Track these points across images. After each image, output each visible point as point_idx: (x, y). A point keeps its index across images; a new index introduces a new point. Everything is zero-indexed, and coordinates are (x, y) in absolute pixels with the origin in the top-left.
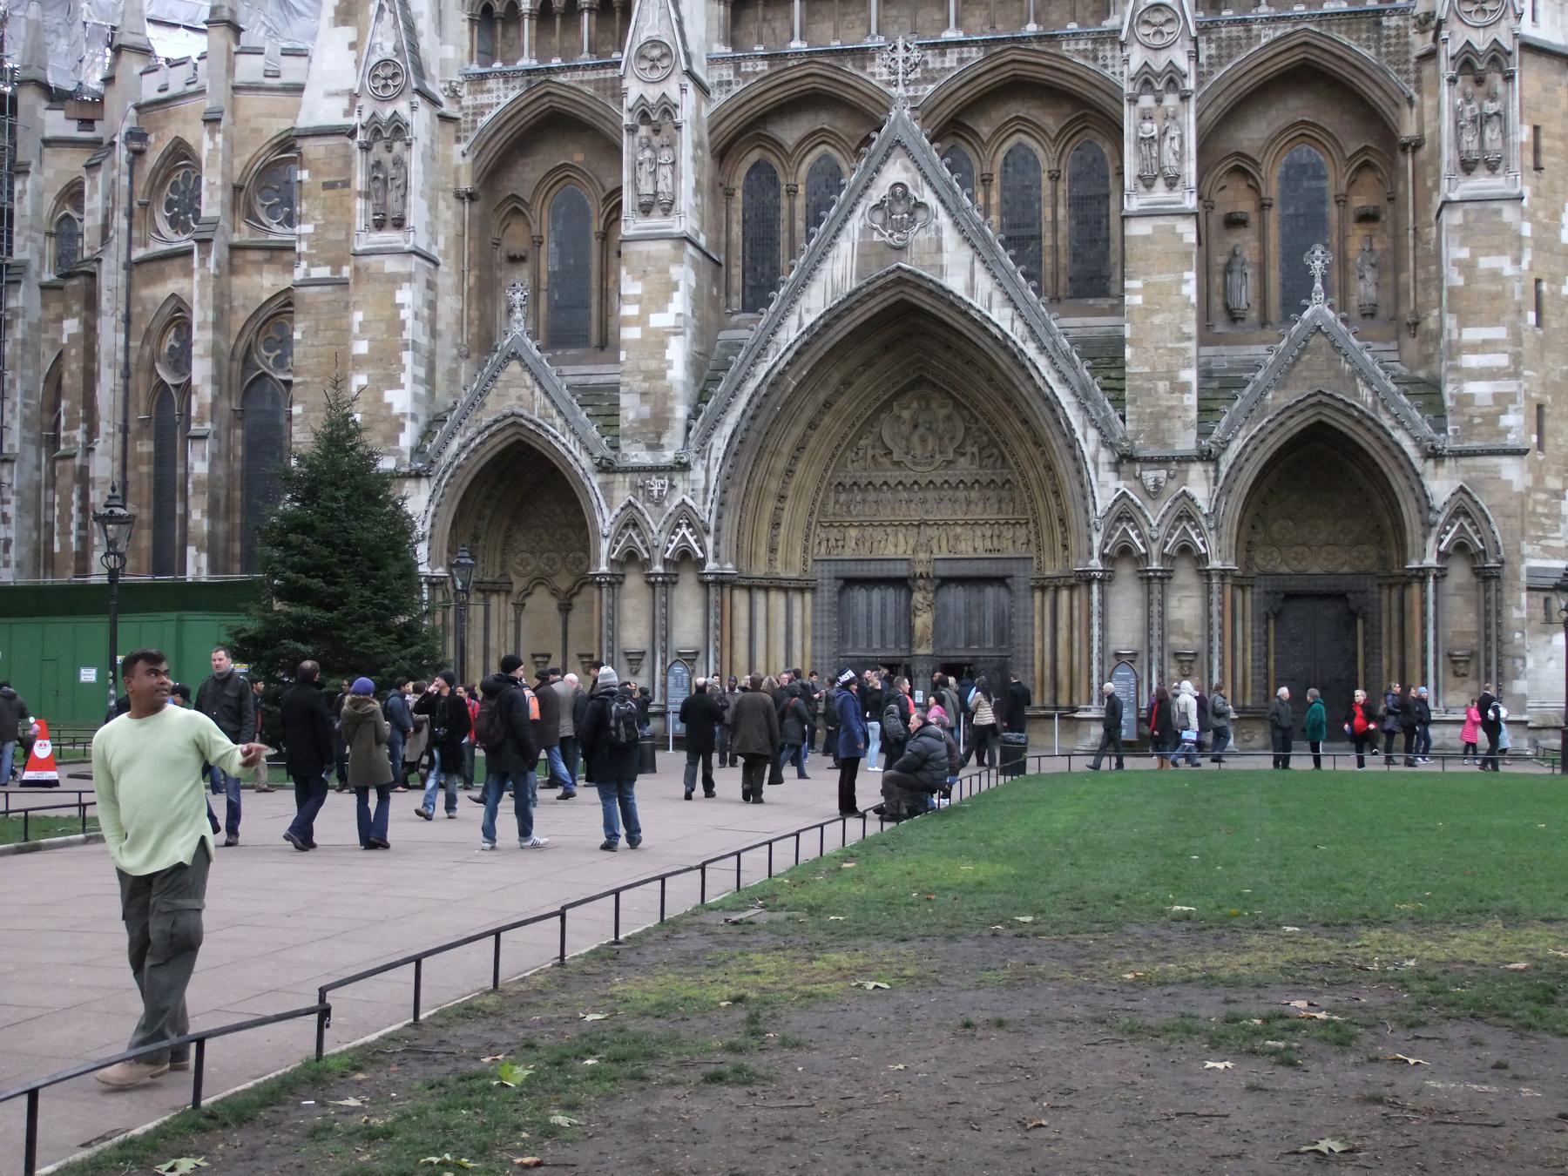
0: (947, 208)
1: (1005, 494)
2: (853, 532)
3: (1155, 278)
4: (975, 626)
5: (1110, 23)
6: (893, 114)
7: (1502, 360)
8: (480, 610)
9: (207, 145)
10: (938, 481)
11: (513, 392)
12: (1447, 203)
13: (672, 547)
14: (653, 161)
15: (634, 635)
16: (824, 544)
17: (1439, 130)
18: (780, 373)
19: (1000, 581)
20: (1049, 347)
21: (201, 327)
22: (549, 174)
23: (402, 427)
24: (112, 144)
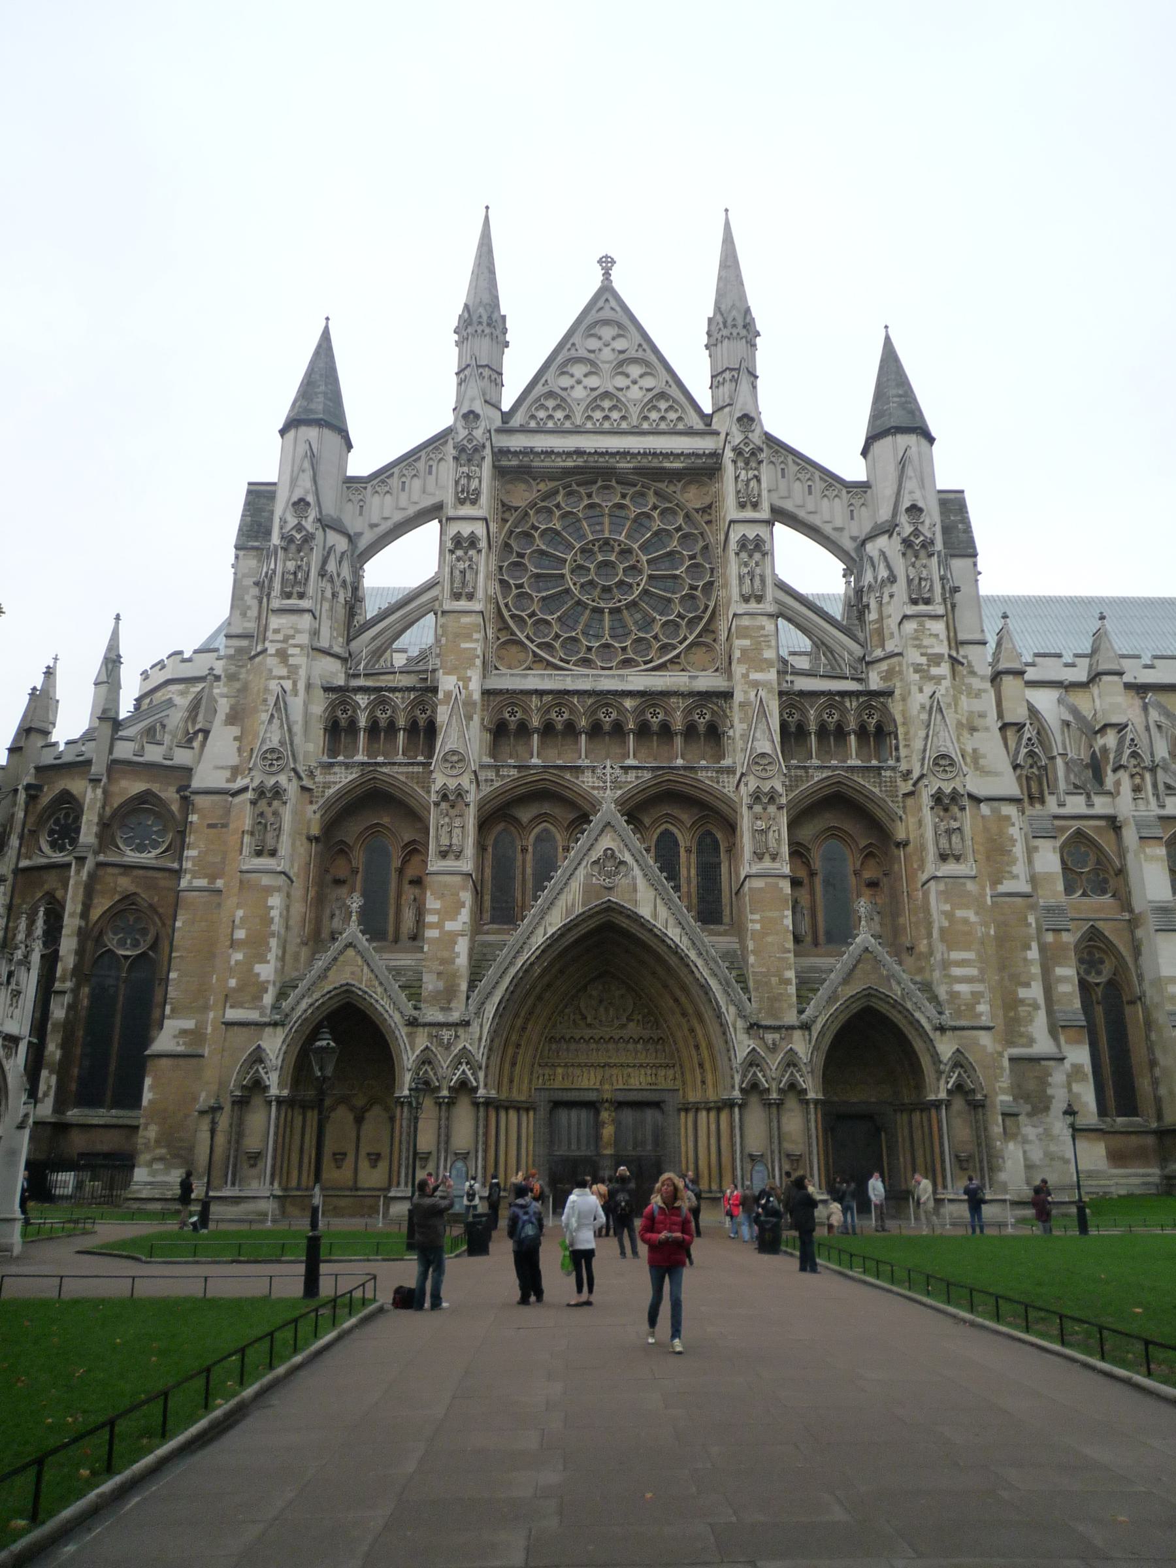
1: (659, 1047)
2: (560, 1070)
3: (769, 914)
5: (726, 762)
6: (604, 805)
7: (973, 972)
8: (301, 1118)
9: (91, 798)
10: (617, 1037)
11: (348, 969)
12: (934, 878)
13: (455, 1078)
15: (426, 1140)
16: (541, 1078)
17: (922, 836)
19: (657, 1105)
20: (704, 953)
21: (72, 915)
22: (366, 829)
23: (266, 991)
24: (16, 791)
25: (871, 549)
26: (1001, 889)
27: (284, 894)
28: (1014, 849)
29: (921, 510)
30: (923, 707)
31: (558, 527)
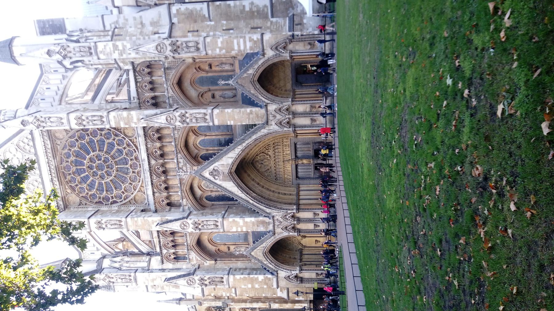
2: (286, 176)
3: (227, 118)
4: (306, 149)
7: (242, 40)
11: (258, 254)
14: (207, 225)
15: (311, 226)
19: (295, 144)
25: (69, 66)
26: (207, 16)
27: (235, 273)
28: (190, 8)
29: (49, 50)
30: (137, 53)
31: (85, 185)
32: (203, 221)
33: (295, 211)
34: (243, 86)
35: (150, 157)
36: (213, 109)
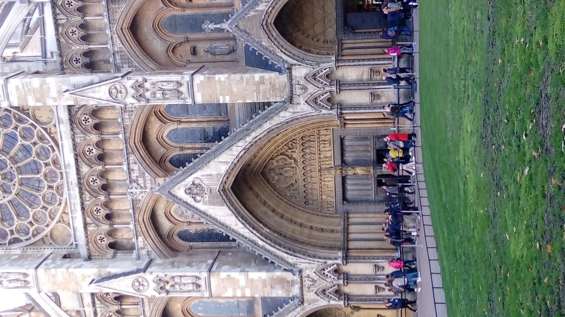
0: (194, 173)
13: (332, 277)
14: (180, 285)
15: (369, 289)
18: (262, 235)
32: (173, 277)
33: (339, 261)
34: (248, 33)
35: (80, 160)
36: (193, 74)
